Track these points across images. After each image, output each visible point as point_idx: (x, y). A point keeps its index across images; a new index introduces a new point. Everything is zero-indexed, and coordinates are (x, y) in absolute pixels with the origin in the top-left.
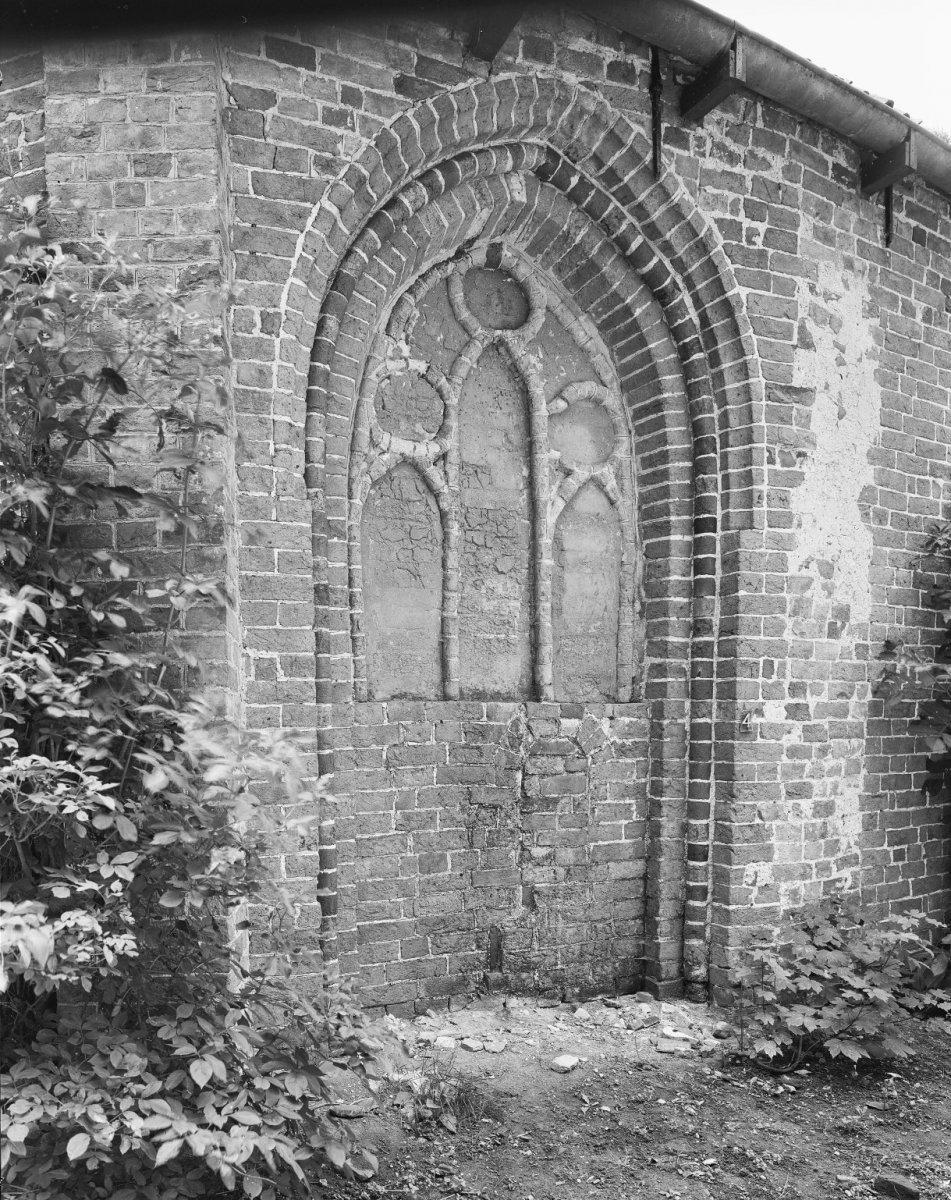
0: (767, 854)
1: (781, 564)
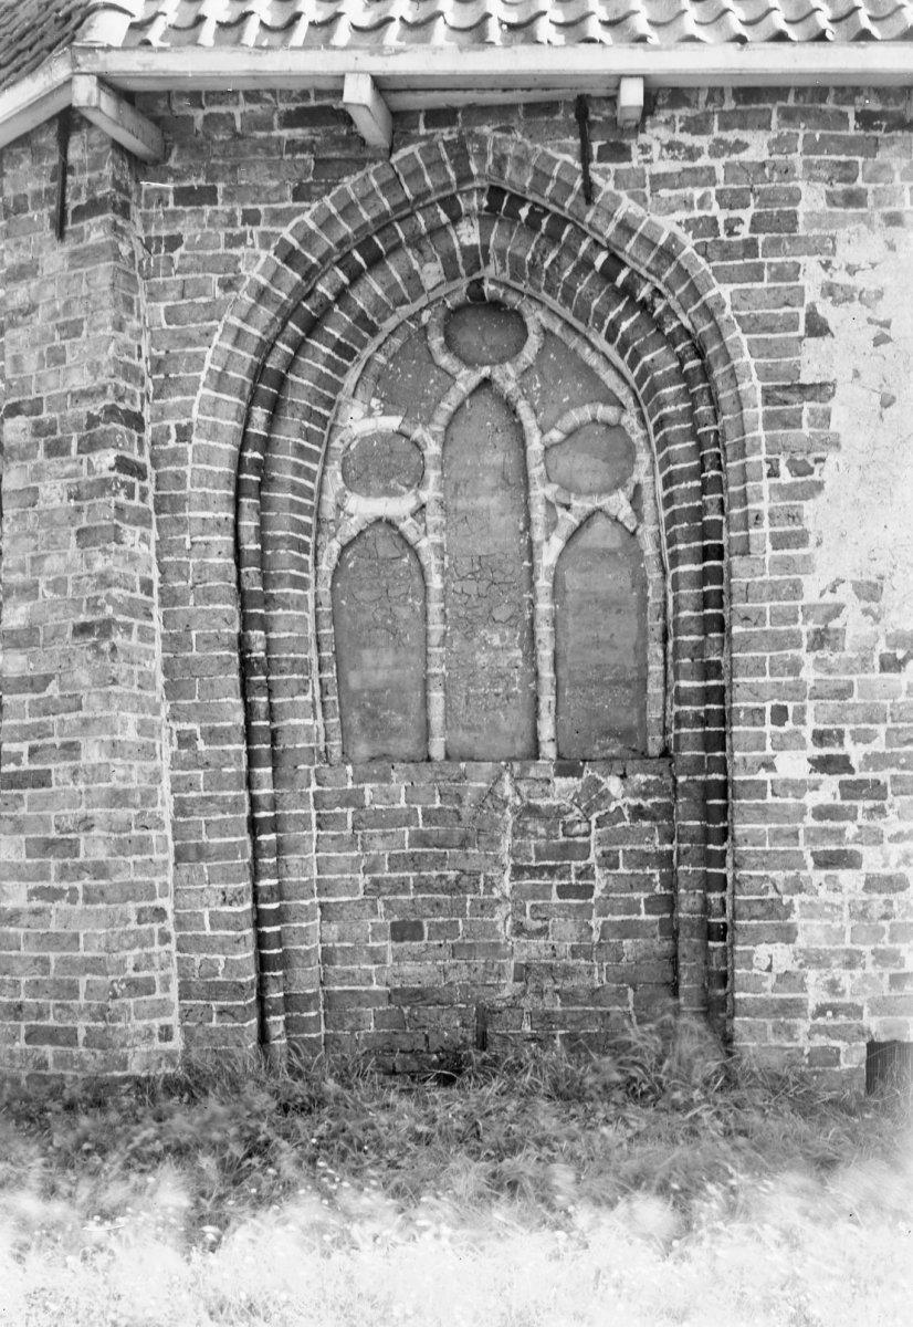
0: (788, 935)
1: (796, 590)
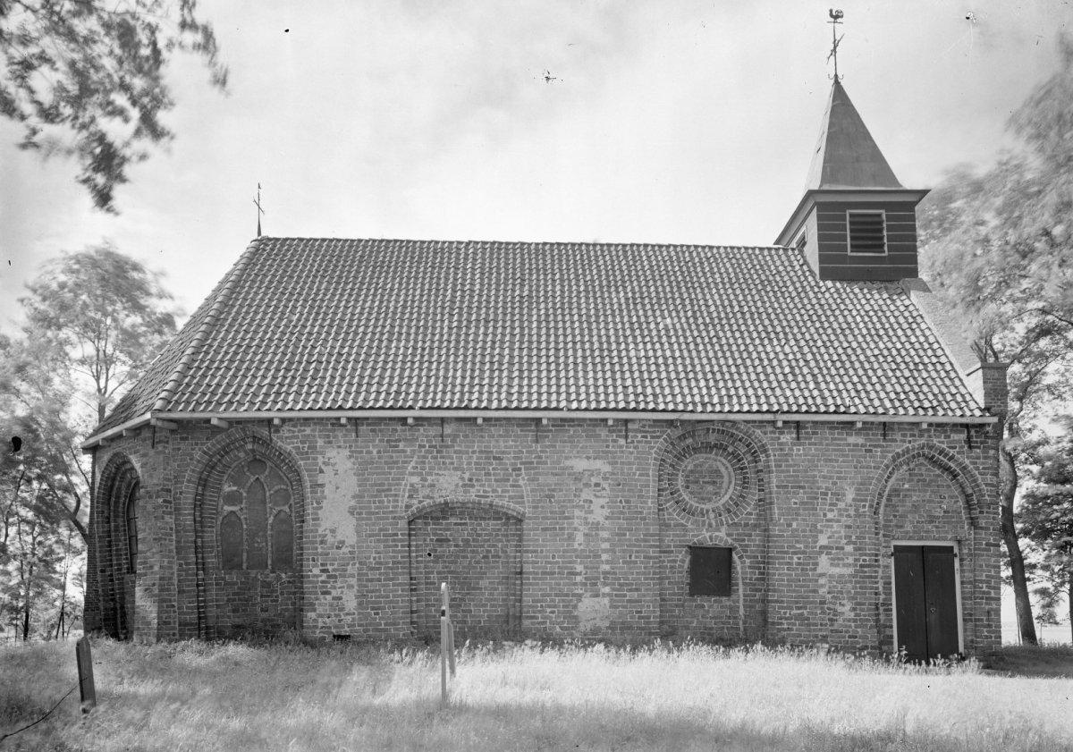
0: (315, 610)
1: (317, 531)
